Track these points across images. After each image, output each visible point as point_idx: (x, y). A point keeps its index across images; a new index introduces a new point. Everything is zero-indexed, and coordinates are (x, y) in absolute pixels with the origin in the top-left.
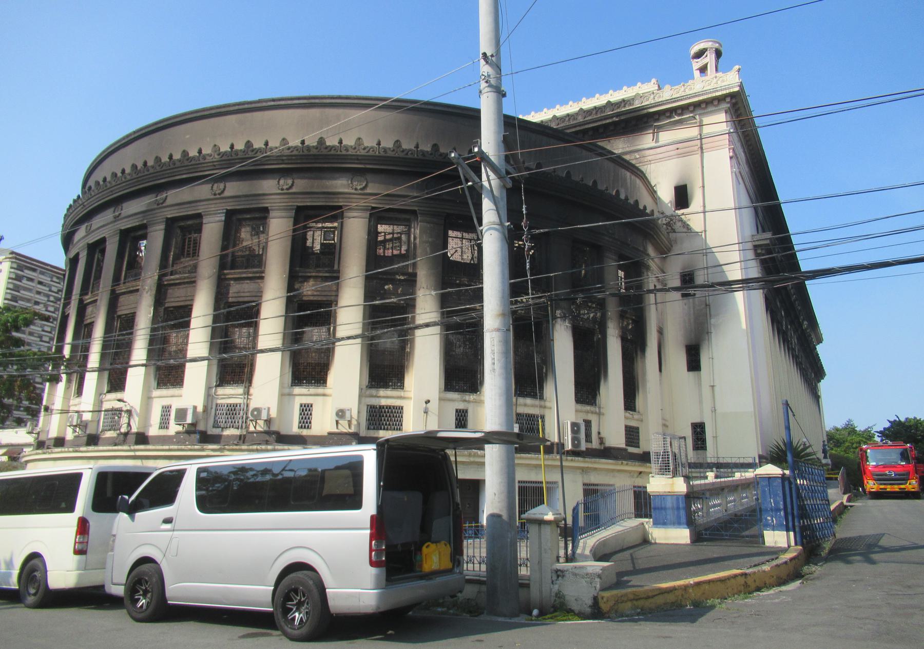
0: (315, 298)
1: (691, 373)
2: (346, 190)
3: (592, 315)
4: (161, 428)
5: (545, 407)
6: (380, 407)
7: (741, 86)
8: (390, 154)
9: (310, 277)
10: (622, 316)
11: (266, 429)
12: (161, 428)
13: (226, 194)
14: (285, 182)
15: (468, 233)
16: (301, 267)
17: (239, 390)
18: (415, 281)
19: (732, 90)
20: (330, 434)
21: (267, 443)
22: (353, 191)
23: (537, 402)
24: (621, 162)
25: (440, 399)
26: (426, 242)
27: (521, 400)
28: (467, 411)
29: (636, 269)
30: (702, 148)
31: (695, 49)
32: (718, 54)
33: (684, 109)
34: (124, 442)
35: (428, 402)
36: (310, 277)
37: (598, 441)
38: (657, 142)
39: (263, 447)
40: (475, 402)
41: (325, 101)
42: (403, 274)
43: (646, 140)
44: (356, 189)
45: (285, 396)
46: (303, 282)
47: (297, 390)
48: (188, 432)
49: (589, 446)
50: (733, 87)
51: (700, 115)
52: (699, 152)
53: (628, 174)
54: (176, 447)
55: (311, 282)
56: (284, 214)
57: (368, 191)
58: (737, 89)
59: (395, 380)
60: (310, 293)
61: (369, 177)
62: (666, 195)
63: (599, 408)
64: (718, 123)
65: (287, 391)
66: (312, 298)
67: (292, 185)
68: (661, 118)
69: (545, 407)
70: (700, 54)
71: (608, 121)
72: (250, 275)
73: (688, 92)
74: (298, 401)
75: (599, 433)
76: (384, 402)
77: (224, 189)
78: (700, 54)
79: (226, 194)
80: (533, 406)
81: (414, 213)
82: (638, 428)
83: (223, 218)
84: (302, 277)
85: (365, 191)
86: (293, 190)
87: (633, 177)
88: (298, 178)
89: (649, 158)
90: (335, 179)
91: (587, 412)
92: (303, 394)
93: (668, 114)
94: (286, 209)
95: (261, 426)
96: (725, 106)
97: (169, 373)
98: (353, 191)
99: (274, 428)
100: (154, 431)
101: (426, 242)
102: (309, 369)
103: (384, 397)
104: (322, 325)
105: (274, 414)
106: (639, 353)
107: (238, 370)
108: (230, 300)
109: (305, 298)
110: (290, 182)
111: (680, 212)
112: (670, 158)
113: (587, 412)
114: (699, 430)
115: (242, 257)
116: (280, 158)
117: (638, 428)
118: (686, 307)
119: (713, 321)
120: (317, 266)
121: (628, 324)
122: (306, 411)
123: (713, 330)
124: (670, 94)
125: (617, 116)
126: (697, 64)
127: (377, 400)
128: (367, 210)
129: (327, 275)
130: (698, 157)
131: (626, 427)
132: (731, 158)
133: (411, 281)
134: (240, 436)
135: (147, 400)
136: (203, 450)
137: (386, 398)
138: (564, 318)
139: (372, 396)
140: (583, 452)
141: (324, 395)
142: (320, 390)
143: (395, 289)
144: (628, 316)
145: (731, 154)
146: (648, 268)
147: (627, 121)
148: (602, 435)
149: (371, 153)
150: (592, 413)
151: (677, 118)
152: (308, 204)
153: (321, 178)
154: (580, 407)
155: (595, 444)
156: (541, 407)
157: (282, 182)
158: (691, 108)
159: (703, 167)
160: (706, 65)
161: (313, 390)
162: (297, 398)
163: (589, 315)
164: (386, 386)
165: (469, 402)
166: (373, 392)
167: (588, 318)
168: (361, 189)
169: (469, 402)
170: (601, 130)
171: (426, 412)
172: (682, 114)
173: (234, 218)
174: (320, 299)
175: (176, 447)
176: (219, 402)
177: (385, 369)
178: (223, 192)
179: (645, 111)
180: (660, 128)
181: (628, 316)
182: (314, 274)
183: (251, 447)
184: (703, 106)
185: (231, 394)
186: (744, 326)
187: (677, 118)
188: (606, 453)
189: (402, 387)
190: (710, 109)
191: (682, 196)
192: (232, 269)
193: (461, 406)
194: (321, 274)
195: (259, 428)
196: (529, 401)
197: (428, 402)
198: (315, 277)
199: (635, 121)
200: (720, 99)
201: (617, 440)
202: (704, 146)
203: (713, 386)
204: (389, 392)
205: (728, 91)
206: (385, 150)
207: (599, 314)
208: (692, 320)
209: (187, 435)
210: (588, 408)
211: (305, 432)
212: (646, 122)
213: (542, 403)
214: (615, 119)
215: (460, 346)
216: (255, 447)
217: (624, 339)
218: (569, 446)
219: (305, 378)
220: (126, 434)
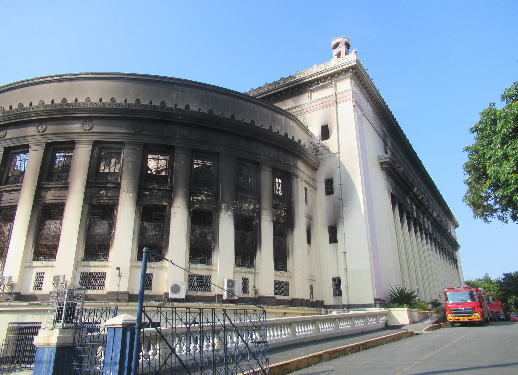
0: (54, 201)
1: (332, 244)
2: (79, 131)
3: (252, 207)
5: (212, 270)
6: (90, 273)
8: (108, 106)
9: (52, 188)
10: (275, 207)
11: (10, 291)
13: (7, 137)
14: (41, 128)
15: (161, 155)
16: (47, 181)
18: (120, 188)
19: (352, 64)
21: (8, 300)
22: (84, 131)
23: (205, 267)
24: (286, 113)
25: (131, 267)
26: (129, 162)
27: (193, 266)
28: (152, 275)
29: (288, 177)
30: (336, 101)
31: (334, 43)
32: (348, 46)
33: (325, 78)
35: (118, 269)
36: (52, 188)
37: (253, 292)
38: (311, 99)
39: (7, 304)
40: (158, 267)
41: (72, 77)
42: (112, 183)
43: (304, 100)
44: (85, 130)
45: (25, 268)
46: (47, 191)
47: (36, 264)
49: (246, 295)
51: (335, 81)
52: (335, 104)
53: (283, 118)
55: (52, 192)
57: (93, 130)
59: (102, 254)
60: (50, 198)
61: (95, 122)
62: (316, 132)
63: (255, 269)
64: (346, 85)
65: (28, 264)
66: (51, 202)
67: (46, 129)
68: (313, 85)
69: (212, 270)
70: (336, 46)
71: (281, 89)
72: (15, 188)
73: (327, 68)
74: (36, 271)
75: (254, 287)
76: (93, 270)
77: (6, 135)
78: (336, 46)
79: (7, 137)
80: (202, 269)
81: (123, 143)
82: (288, 283)
83: (2, 153)
84: (46, 188)
86: (46, 132)
87: (287, 120)
88: (52, 125)
89: (306, 110)
90: (73, 124)
91: (245, 272)
92: (39, 266)
93: (316, 82)
94: (40, 144)
95: (7, 290)
96: (349, 74)
98: (84, 131)
99: (16, 290)
101: (129, 162)
102: (44, 248)
103: (93, 266)
104: (58, 219)
105: (15, 280)
106: (290, 232)
109: (47, 202)
110: (44, 127)
111: (323, 142)
112: (318, 109)
113: (245, 272)
114: (337, 281)
115: (13, 176)
116: (38, 113)
117: (288, 283)
118: (328, 202)
119: (344, 210)
120: (58, 180)
121: (281, 213)
122: (40, 277)
123: (344, 216)
124: (315, 70)
125: (286, 86)
126: (335, 52)
127: (88, 268)
128: (91, 143)
129: (63, 186)
130: (334, 107)
131: (276, 282)
132: (354, 106)
133: (117, 187)
137: (95, 267)
138: (228, 209)
139: (85, 266)
140: (236, 300)
141: (52, 266)
142: (50, 263)
143: (107, 194)
144: (280, 207)
145: (354, 104)
146: (297, 176)
147: (293, 89)
148: (256, 288)
149: (95, 106)
150: (249, 273)
151: (321, 84)
152: (54, 141)
153: (64, 124)
154: (238, 269)
155: (251, 294)
156: (208, 270)
157: (39, 128)
158: (329, 78)
159: (337, 113)
160: (340, 52)
161: (45, 263)
163: (249, 207)
164: (96, 259)
165: (154, 268)
166: (86, 263)
167: (249, 209)
168: (89, 130)
169: (154, 268)
170: (278, 95)
171: (120, 276)
172: (324, 82)
173: (11, 152)
174: (56, 201)
177: (96, 247)
178: (4, 136)
179: (302, 82)
180: (312, 91)
181: (280, 207)
182: (54, 186)
184: (336, 75)
186: (363, 212)
187: (321, 84)
188: (259, 301)
189: (107, 259)
190: (341, 77)
191: (325, 132)
192: (5, 185)
194: (58, 186)
195: (5, 291)
196: (199, 266)
199: (297, 88)
200: (346, 71)
201: (267, 289)
202: (338, 100)
203: (345, 253)
204: (97, 263)
205: (349, 65)
206: (104, 105)
207: (257, 207)
208: (332, 210)
210: (246, 269)
211: (37, 293)
212: (304, 88)
213: (209, 267)
214: (285, 88)
215: (152, 230)
217: (276, 224)
218: (225, 297)
219: (42, 255)
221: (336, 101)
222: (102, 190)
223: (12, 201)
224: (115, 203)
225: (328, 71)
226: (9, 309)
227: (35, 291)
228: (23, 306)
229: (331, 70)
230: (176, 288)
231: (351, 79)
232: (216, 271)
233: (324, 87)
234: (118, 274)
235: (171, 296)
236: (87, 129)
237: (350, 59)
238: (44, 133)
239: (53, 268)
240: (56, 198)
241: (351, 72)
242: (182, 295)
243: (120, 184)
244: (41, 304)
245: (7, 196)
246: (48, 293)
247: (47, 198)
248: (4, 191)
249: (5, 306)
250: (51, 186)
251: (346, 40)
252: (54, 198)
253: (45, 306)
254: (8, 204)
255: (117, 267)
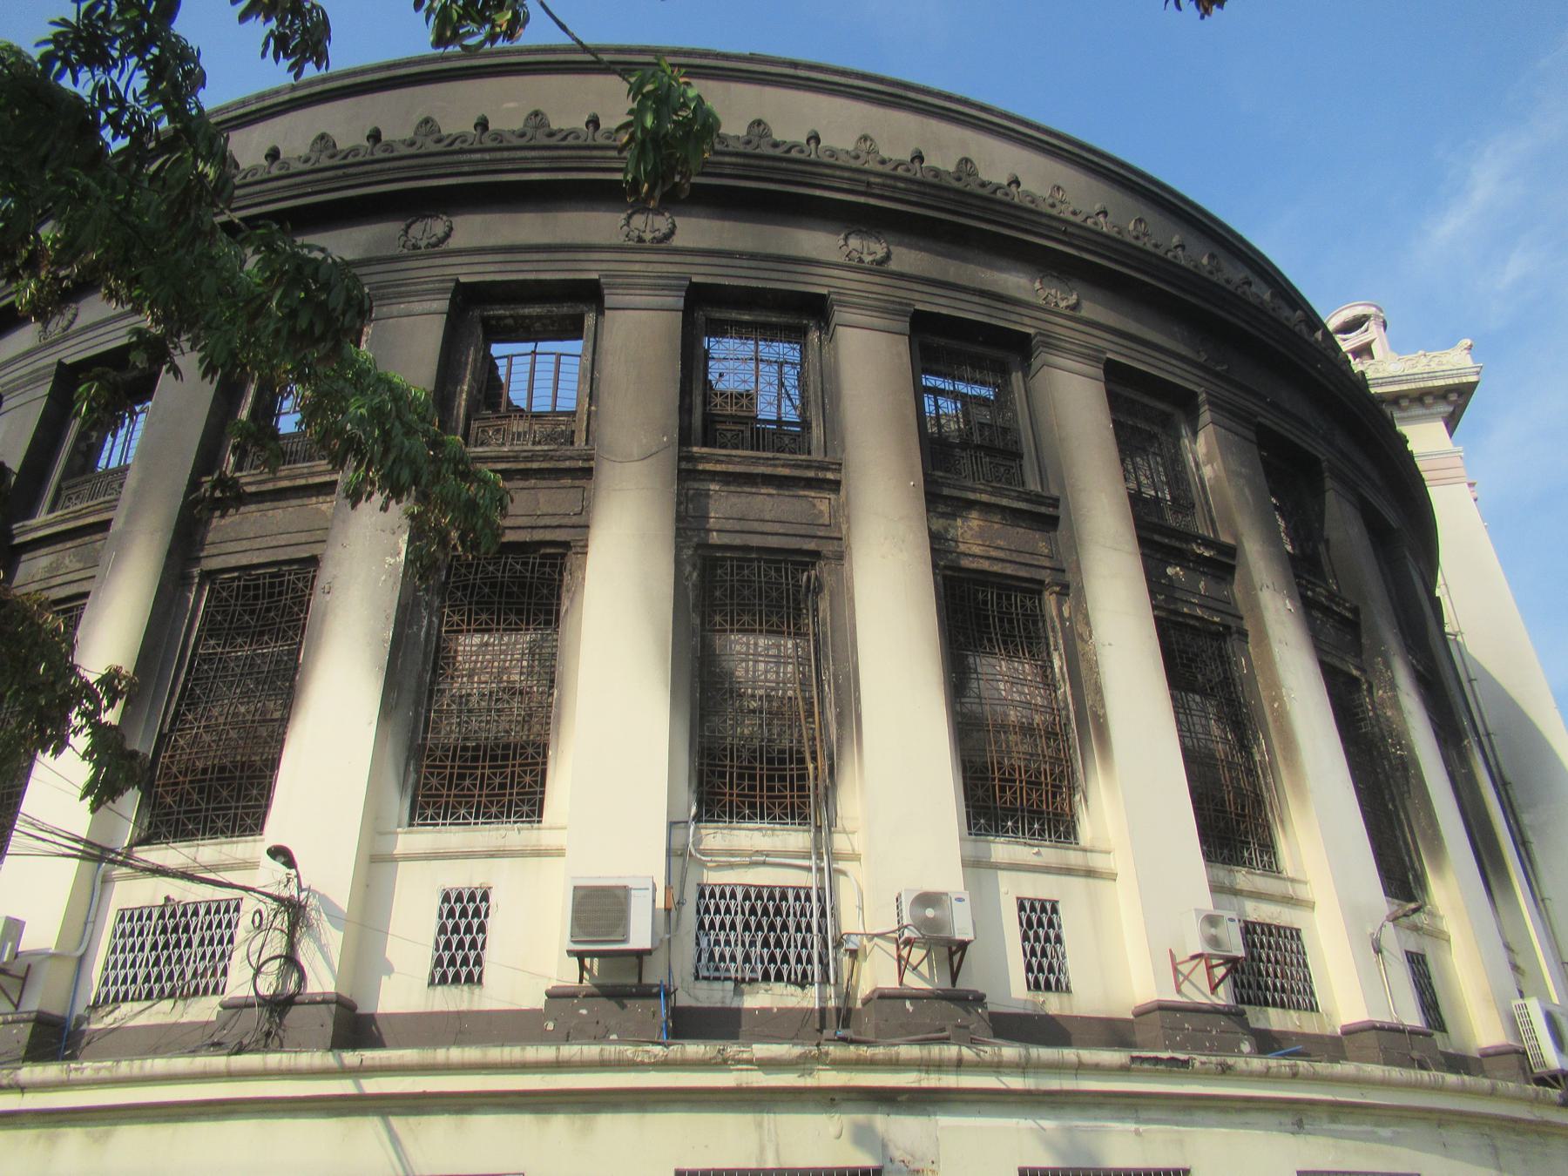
0: (997, 568)
4: (439, 979)
9: (971, 505)
11: (941, 982)
12: (439, 979)
17: (795, 839)
34: (268, 1040)
42: (1208, 543)
46: (953, 516)
48: (613, 993)
54: (592, 1051)
55: (974, 521)
56: (877, 322)
60: (976, 550)
72: (786, 472)
74: (1011, 889)
85: (1078, 314)
88: (910, 246)
90: (1001, 270)
97: (470, 764)
100: (403, 988)
107: (761, 769)
108: (714, 538)
109: (966, 563)
134: (823, 1011)
135: (376, 862)
136: (721, 1064)
152: (944, 311)
153: (965, 260)
162: (1003, 876)
174: (1009, 570)
175: (547, 1053)
176: (713, 878)
182: (984, 498)
183: (936, 1051)
185: (758, 854)
194: (1005, 502)
198: (986, 508)
209: (611, 1005)
211: (1053, 1004)
216: (951, 1051)
219: (1011, 813)
220: (279, 1005)
222: (1170, 564)
223: (778, 528)
224: (1227, 628)
226: (1015, 1082)
227: (1041, 997)
228: (1098, 1070)
239: (1090, 881)
240: (1001, 554)
243: (1231, 551)
244: (1185, 1063)
245: (734, 499)
247: (962, 548)
248: (713, 476)
249: (997, 1067)
250: (971, 496)
252: (994, 553)
253: (1205, 1074)
254: (755, 541)
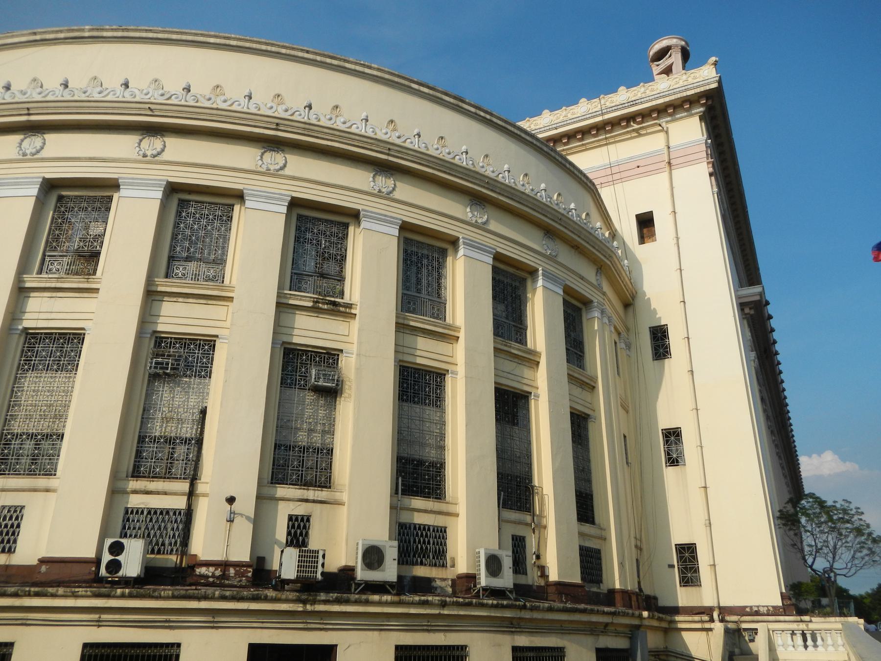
7: (720, 82)
19: (707, 88)
20: (43, 561)
28: (308, 520)
30: (669, 163)
31: (657, 47)
32: (686, 55)
35: (231, 500)
50: (708, 84)
52: (667, 169)
58: (715, 85)
64: (690, 131)
70: (662, 54)
78: (662, 54)
142: (41, 482)
187: (636, 126)
193: (300, 510)
197: (231, 500)
205: (702, 89)
221: (669, 163)
225: (652, 100)
229: (660, 97)
230: (373, 556)
231: (701, 119)
232: (457, 515)
233: (638, 134)
234: (226, 515)
235: (361, 574)
236: (149, 153)
237: (705, 76)
238: (36, 156)
241: (702, 105)
242: (389, 572)
246: (35, 562)
251: (683, 43)
255: (228, 495)
